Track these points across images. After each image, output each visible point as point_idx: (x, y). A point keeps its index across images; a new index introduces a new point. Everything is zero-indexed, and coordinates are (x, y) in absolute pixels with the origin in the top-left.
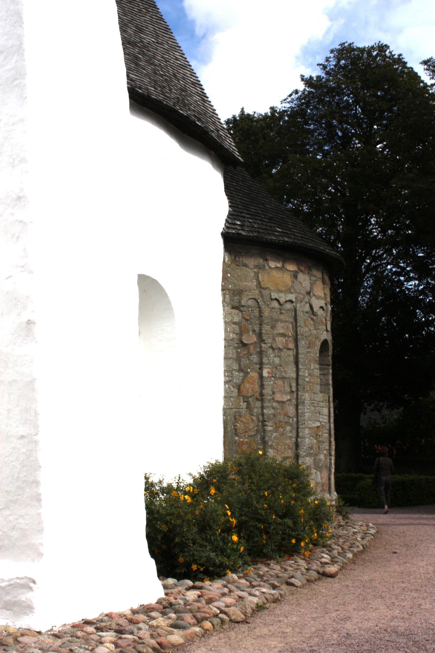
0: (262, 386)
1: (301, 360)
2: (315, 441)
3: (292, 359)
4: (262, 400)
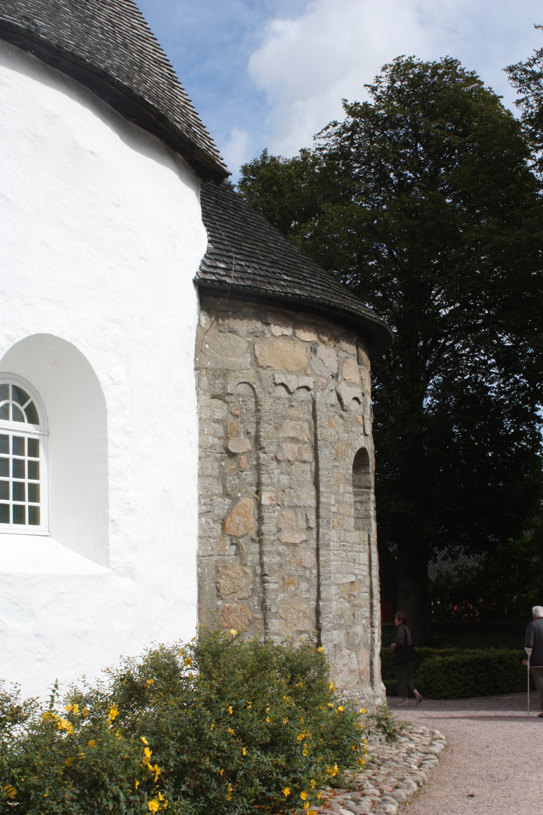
0: (260, 519)
1: (323, 479)
2: (348, 604)
3: (309, 477)
4: (260, 542)
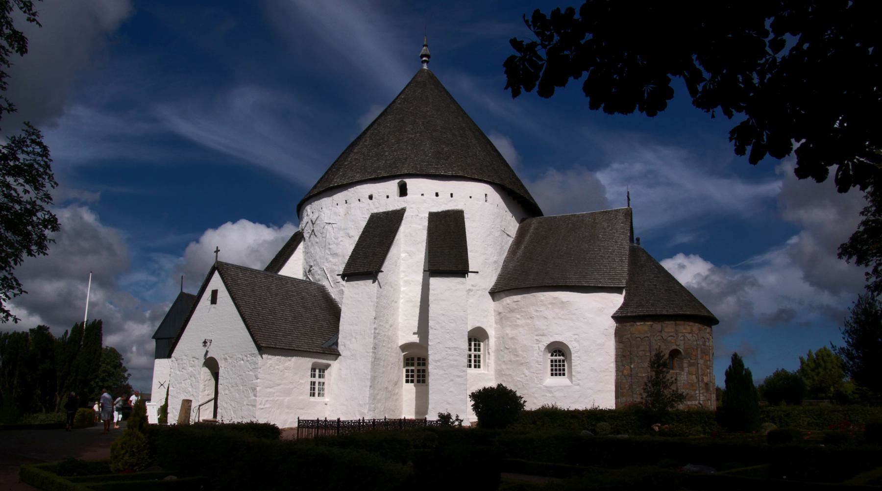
4: (631, 377)
